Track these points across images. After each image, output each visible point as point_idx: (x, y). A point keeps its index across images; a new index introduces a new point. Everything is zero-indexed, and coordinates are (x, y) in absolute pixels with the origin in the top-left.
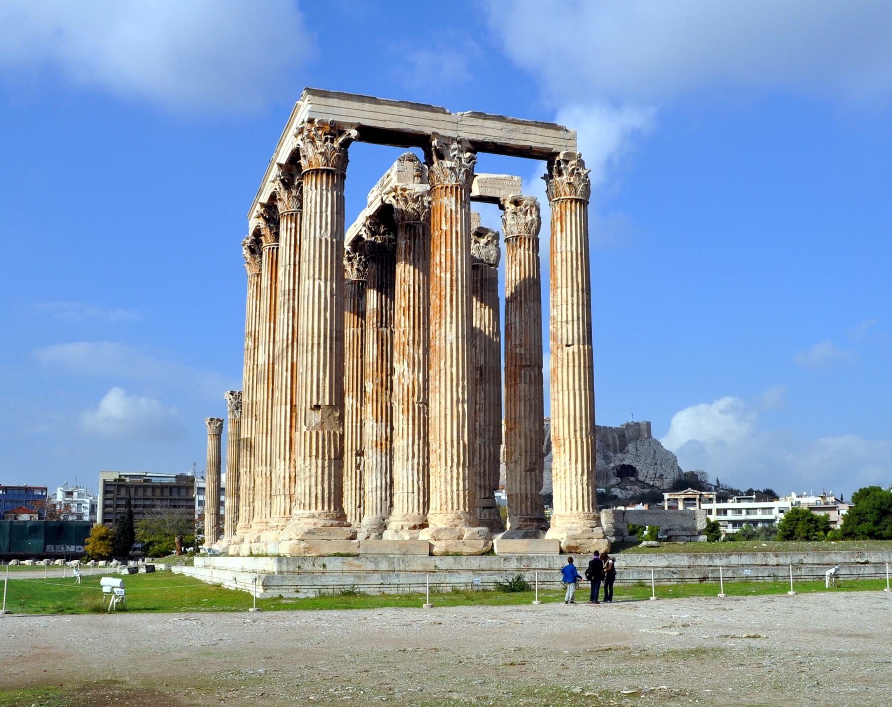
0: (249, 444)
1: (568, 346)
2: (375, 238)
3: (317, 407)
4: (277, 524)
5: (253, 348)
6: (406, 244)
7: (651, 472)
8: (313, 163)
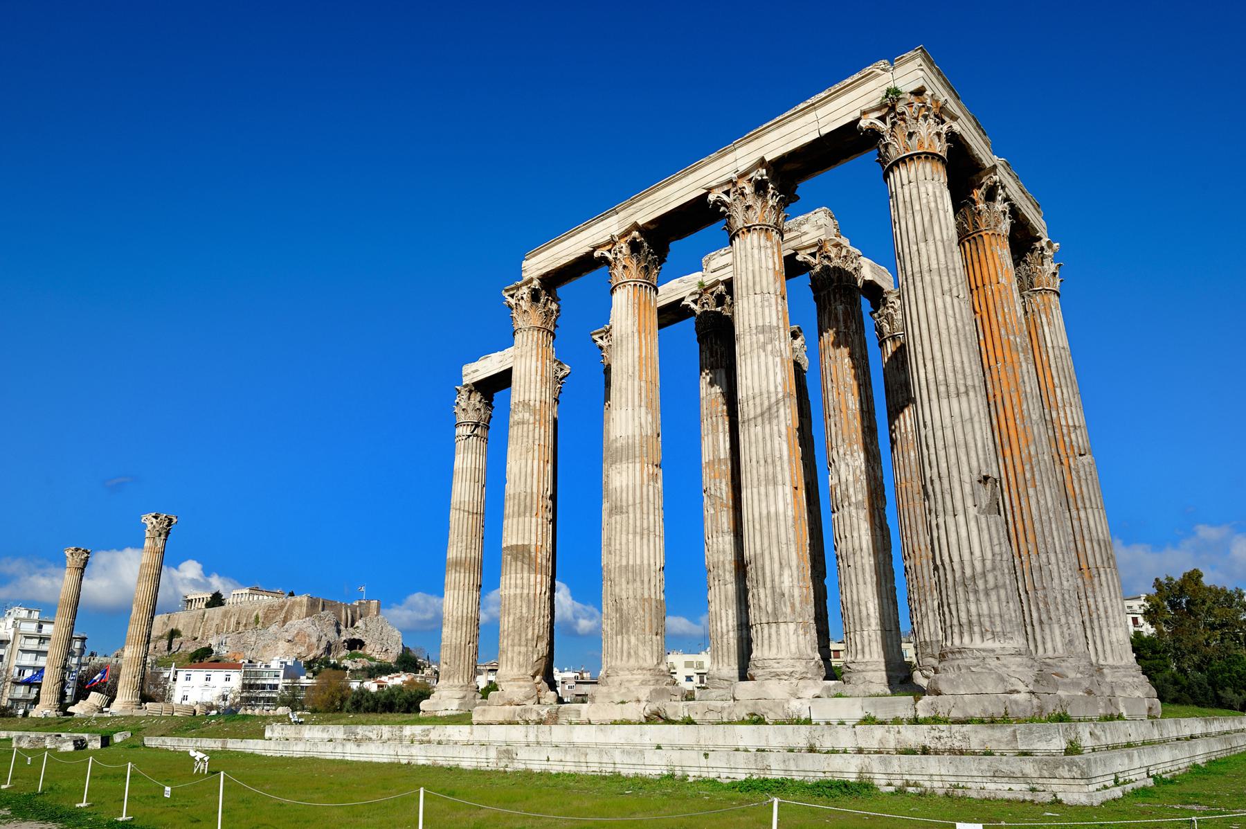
0: (527, 555)
1: (1081, 455)
2: (722, 310)
3: (986, 478)
4: (791, 670)
5: (532, 421)
6: (846, 308)
7: (378, 647)
8: (926, 145)
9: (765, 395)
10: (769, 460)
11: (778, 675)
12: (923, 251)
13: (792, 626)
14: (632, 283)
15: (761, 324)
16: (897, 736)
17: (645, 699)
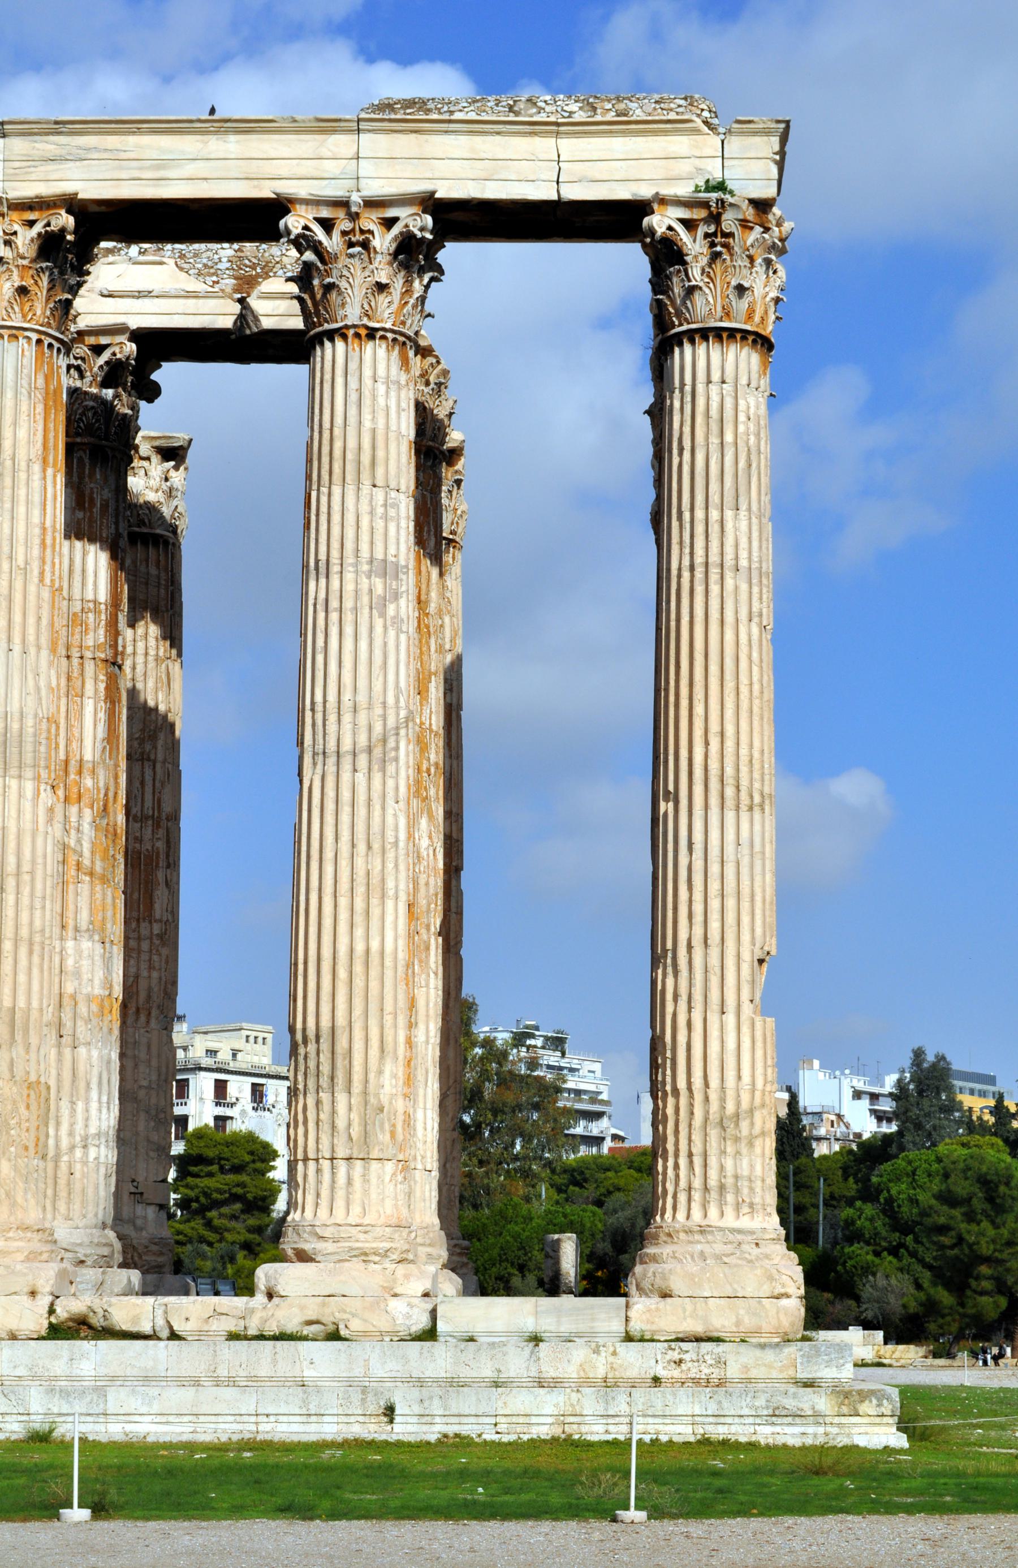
4: (387, 1245)
9: (378, 711)
10: (376, 846)
11: (366, 1254)
12: (729, 526)
13: (390, 1167)
14: (34, 337)
15: (379, 555)
16: (611, 1359)
17: (48, 1289)
